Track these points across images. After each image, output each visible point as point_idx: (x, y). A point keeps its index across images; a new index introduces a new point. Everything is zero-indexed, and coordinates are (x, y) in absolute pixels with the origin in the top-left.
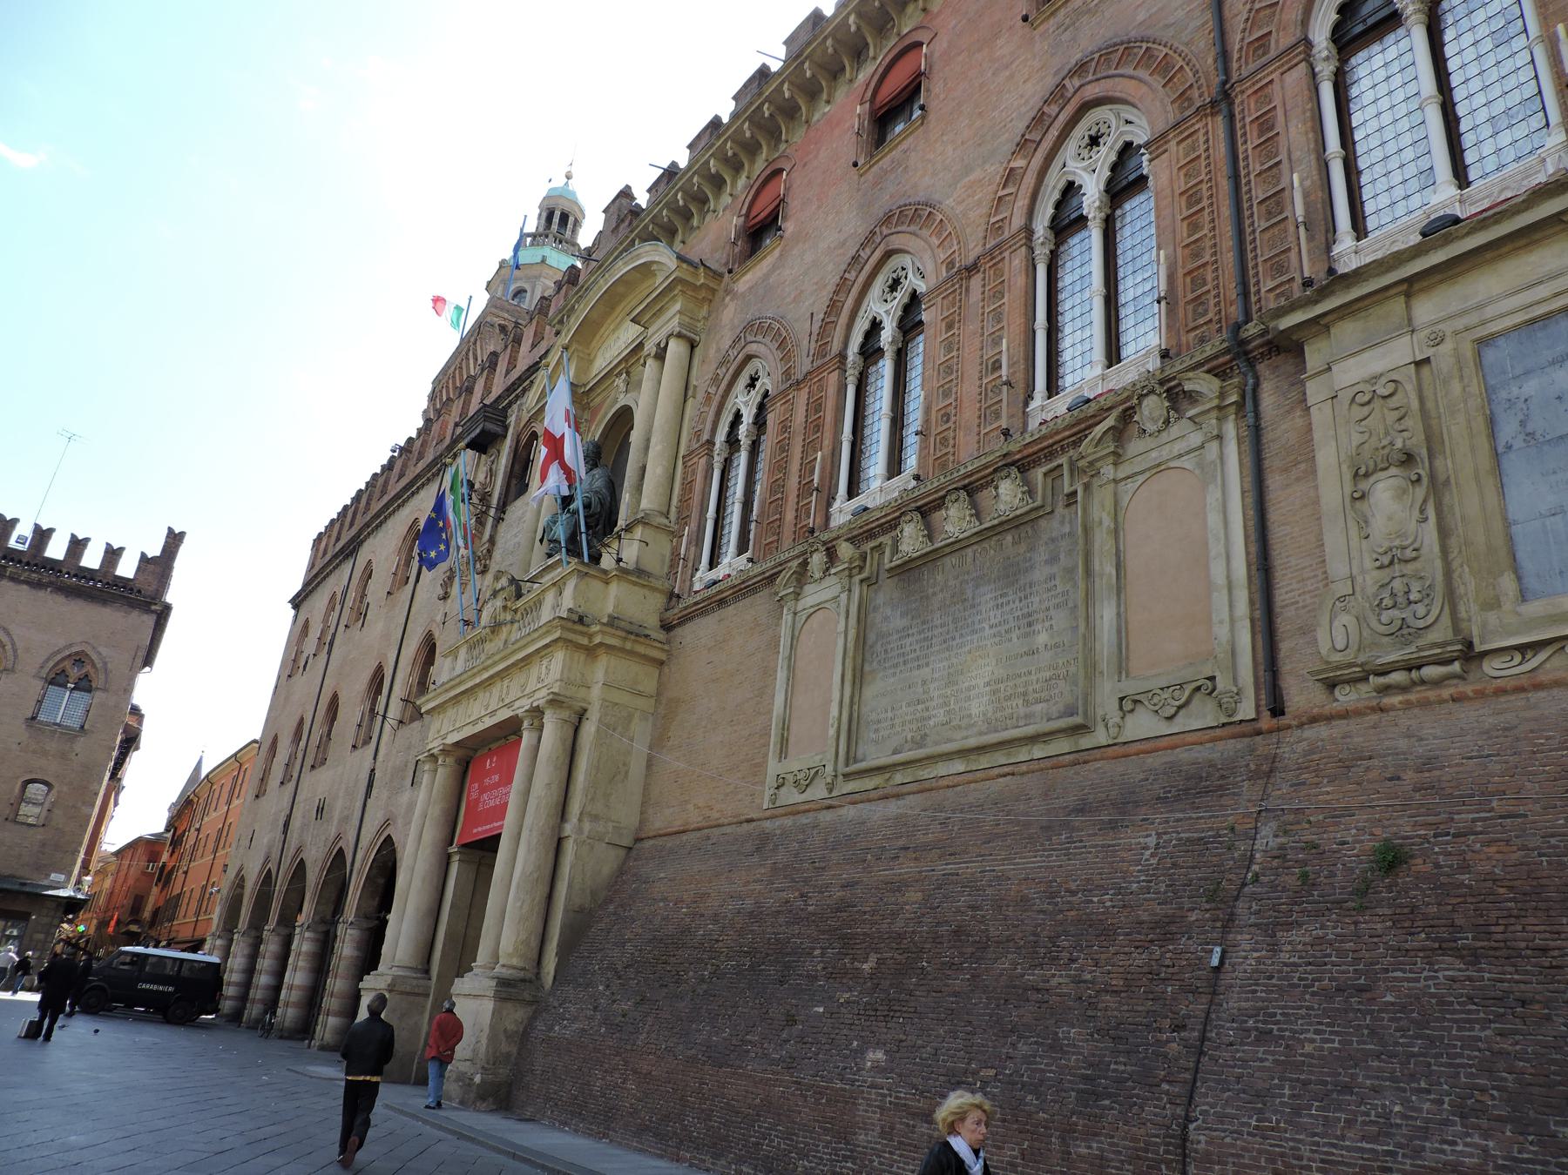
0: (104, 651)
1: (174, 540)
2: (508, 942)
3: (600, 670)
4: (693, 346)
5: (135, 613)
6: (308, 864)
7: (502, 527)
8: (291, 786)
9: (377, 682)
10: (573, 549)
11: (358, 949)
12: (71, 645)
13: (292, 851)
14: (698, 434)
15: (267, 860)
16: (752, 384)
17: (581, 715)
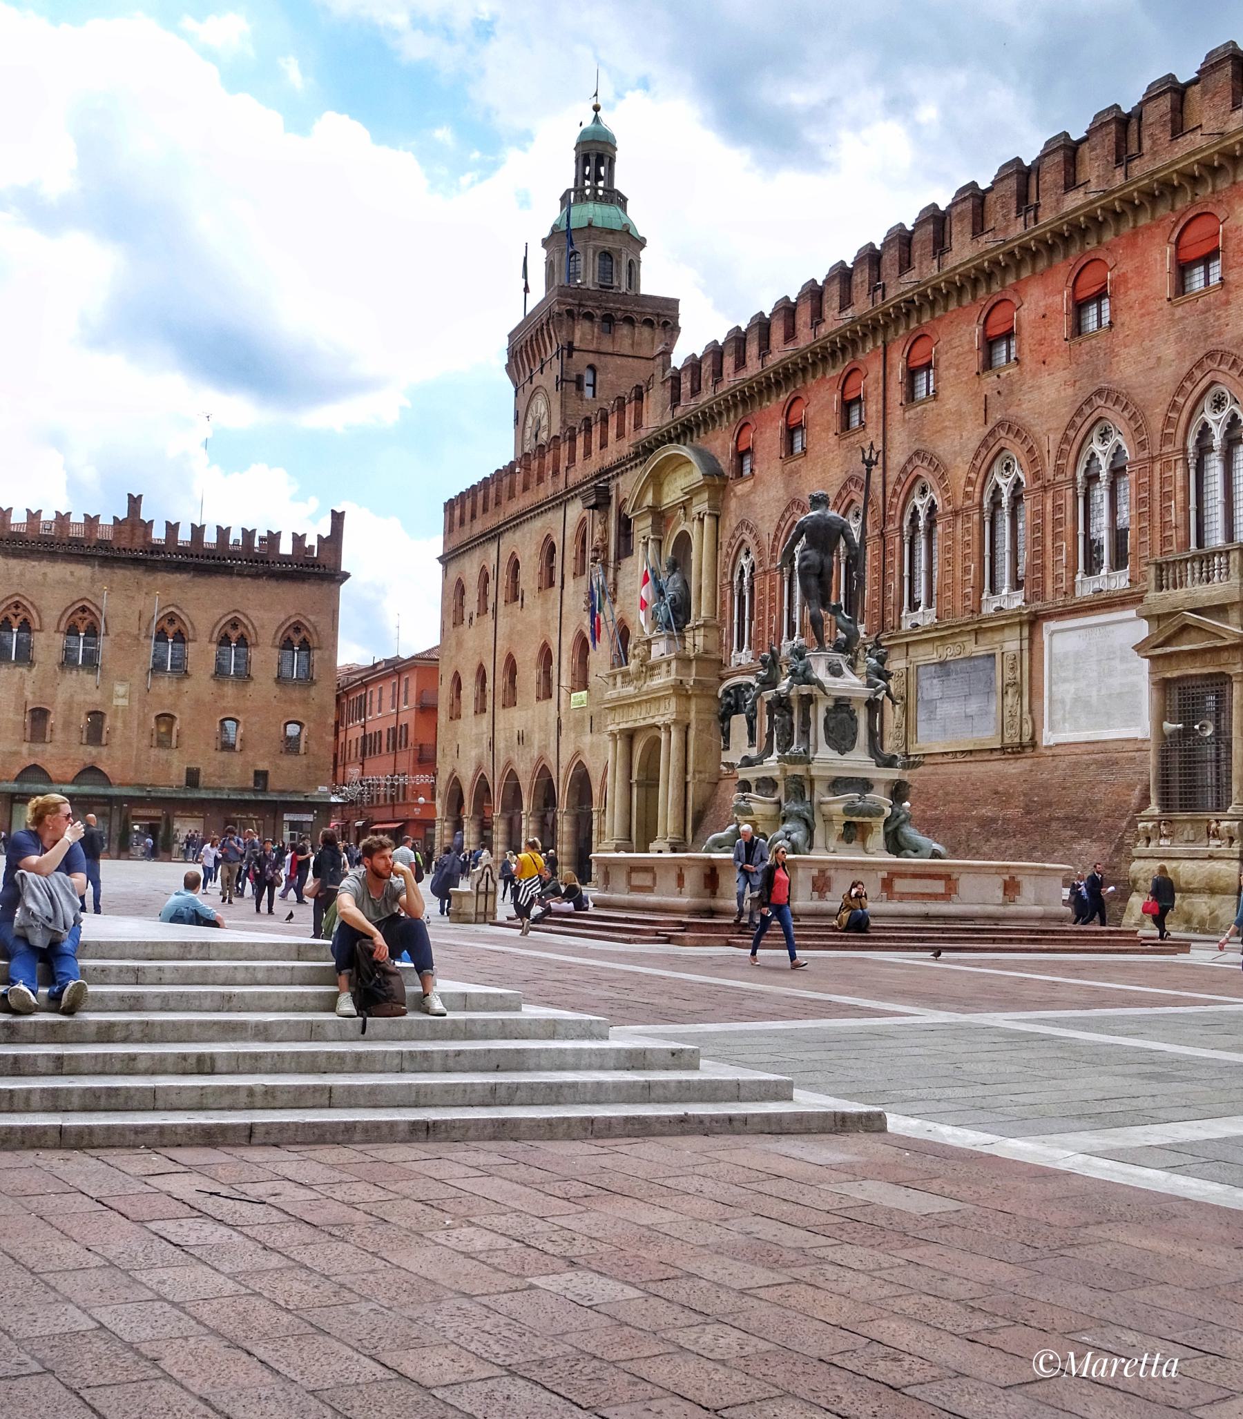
0: (312, 618)
1: (338, 519)
2: (670, 828)
4: (717, 517)
5: (326, 584)
6: (520, 774)
7: (620, 574)
8: (487, 717)
9: (546, 656)
10: (668, 627)
11: (571, 826)
12: (290, 617)
13: (502, 764)
14: (725, 574)
15: (479, 768)
16: (747, 553)
17: (688, 727)
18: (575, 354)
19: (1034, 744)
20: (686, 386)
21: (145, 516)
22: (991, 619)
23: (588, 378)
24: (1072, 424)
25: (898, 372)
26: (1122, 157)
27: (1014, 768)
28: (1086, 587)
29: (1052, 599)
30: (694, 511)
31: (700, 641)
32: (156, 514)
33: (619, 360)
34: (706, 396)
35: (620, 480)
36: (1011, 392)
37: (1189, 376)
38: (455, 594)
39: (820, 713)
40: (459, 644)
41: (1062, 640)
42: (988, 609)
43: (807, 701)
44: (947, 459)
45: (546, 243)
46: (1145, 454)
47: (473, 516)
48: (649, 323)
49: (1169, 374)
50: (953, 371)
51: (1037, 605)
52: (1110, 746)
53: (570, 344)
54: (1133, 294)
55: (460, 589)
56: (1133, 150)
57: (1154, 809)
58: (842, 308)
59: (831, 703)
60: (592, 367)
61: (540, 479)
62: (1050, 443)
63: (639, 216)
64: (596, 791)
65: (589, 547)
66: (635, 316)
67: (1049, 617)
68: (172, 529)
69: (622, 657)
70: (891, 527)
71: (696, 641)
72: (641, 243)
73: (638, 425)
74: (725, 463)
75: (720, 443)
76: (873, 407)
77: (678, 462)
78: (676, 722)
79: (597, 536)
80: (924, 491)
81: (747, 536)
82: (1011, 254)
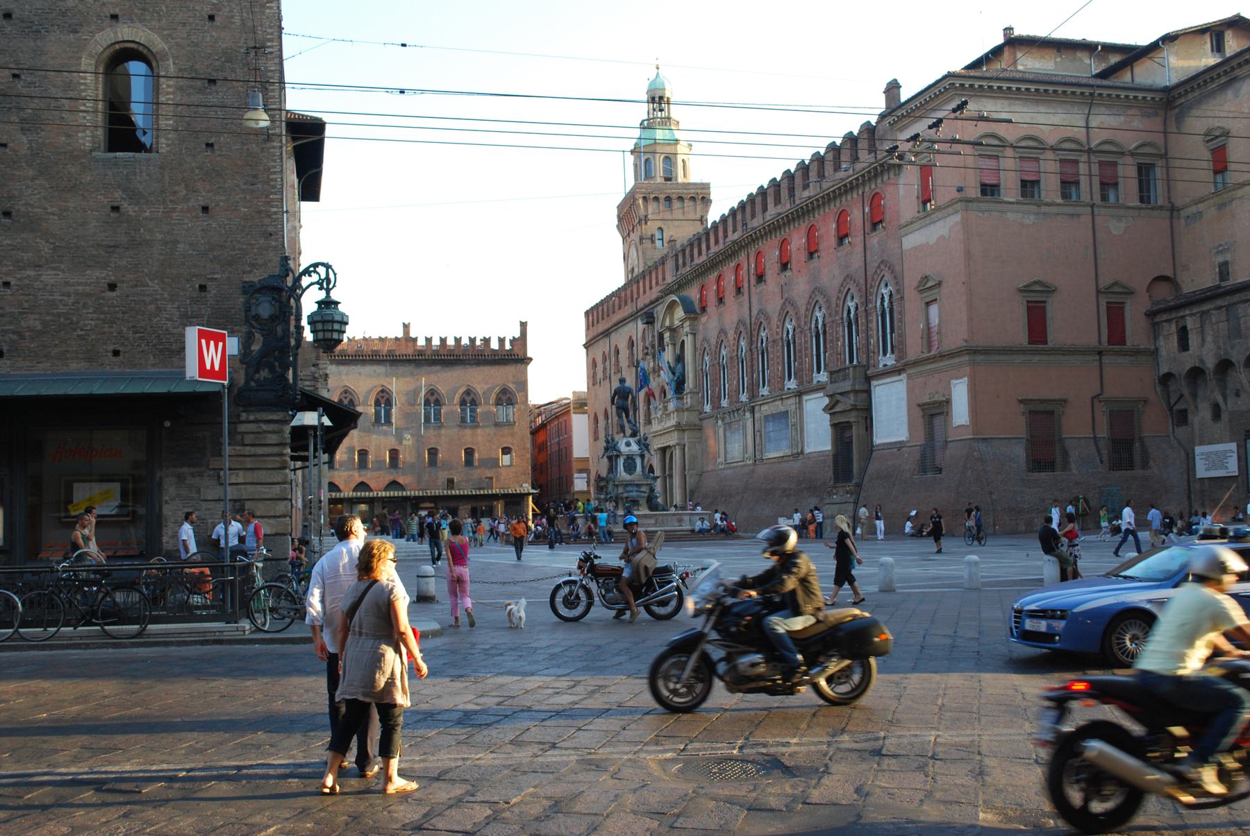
1: (523, 325)
3: (686, 435)
19: (802, 452)
21: (413, 335)
23: (658, 235)
32: (420, 334)
33: (676, 223)
38: (592, 365)
39: (621, 461)
43: (617, 456)
49: (837, 282)
60: (660, 229)
61: (626, 304)
68: (429, 340)
71: (688, 401)
73: (664, 279)
75: (693, 293)
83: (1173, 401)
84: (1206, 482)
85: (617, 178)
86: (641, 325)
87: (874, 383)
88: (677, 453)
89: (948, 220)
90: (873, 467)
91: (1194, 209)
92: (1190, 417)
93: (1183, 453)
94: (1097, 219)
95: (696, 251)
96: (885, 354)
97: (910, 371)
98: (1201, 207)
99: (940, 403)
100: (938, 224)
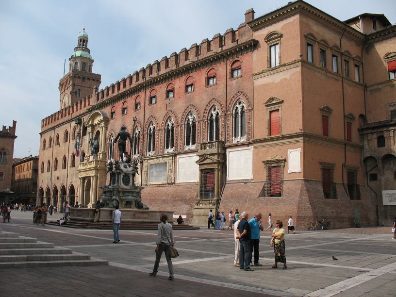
0: (7, 147)
1: (15, 123)
8: (50, 172)
9: (65, 159)
15: (48, 185)
17: (98, 177)
18: (75, 86)
19: (174, 183)
20: (100, 96)
22: (166, 154)
23: (78, 92)
24: (185, 112)
25: (147, 98)
26: (197, 54)
27: (171, 189)
28: (187, 148)
29: (180, 150)
30: (101, 126)
31: (101, 156)
33: (86, 88)
34: (105, 99)
35: (84, 117)
36: (172, 103)
37: (209, 103)
39: (121, 177)
40: (44, 154)
41: (182, 160)
42: (166, 152)
43: (119, 174)
44: (158, 118)
45: (70, 60)
46: (199, 120)
47: (49, 124)
48: (94, 80)
49: (205, 102)
50: (160, 98)
51: (176, 152)
52: (191, 184)
53: (74, 84)
54: (198, 84)
55: (45, 141)
56: (200, 53)
57: (199, 198)
58: (136, 81)
59: (124, 174)
60: (79, 90)
61: (65, 116)
62: (180, 116)
63: (93, 55)
64: (76, 191)
65: (76, 133)
66: (90, 78)
67: (179, 154)
69: (82, 160)
70: (145, 132)
71: (100, 157)
72: (93, 61)
73: (89, 104)
74: (109, 115)
75: (107, 110)
76: (142, 105)
77: (98, 114)
78: (95, 176)
79: (78, 130)
80: (153, 125)
81: (113, 133)
82: (173, 73)
83: (368, 170)
84: (389, 207)
85: (61, 69)
86: (73, 124)
87: (228, 150)
88: (93, 181)
89: (290, 70)
90: (227, 191)
91: (376, 87)
92: (379, 177)
93: (373, 193)
94: (344, 84)
95: (83, 106)
96: (135, 154)
97: (255, 145)
98: (380, 86)
99: (279, 161)
100: (282, 73)
